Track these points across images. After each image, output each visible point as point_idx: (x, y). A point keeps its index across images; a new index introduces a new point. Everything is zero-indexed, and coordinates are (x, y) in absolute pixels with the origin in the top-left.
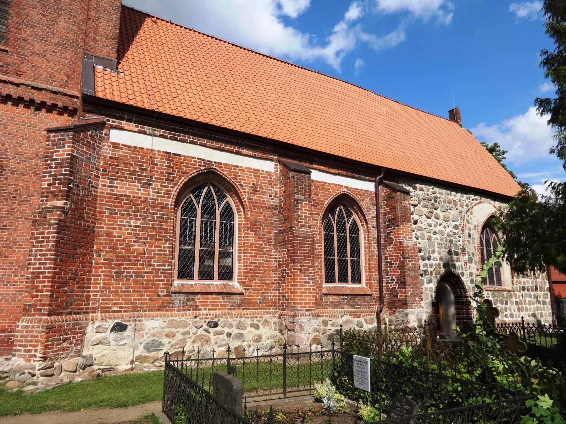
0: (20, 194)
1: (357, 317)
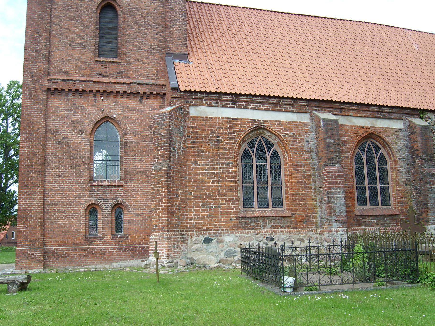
0: (138, 157)
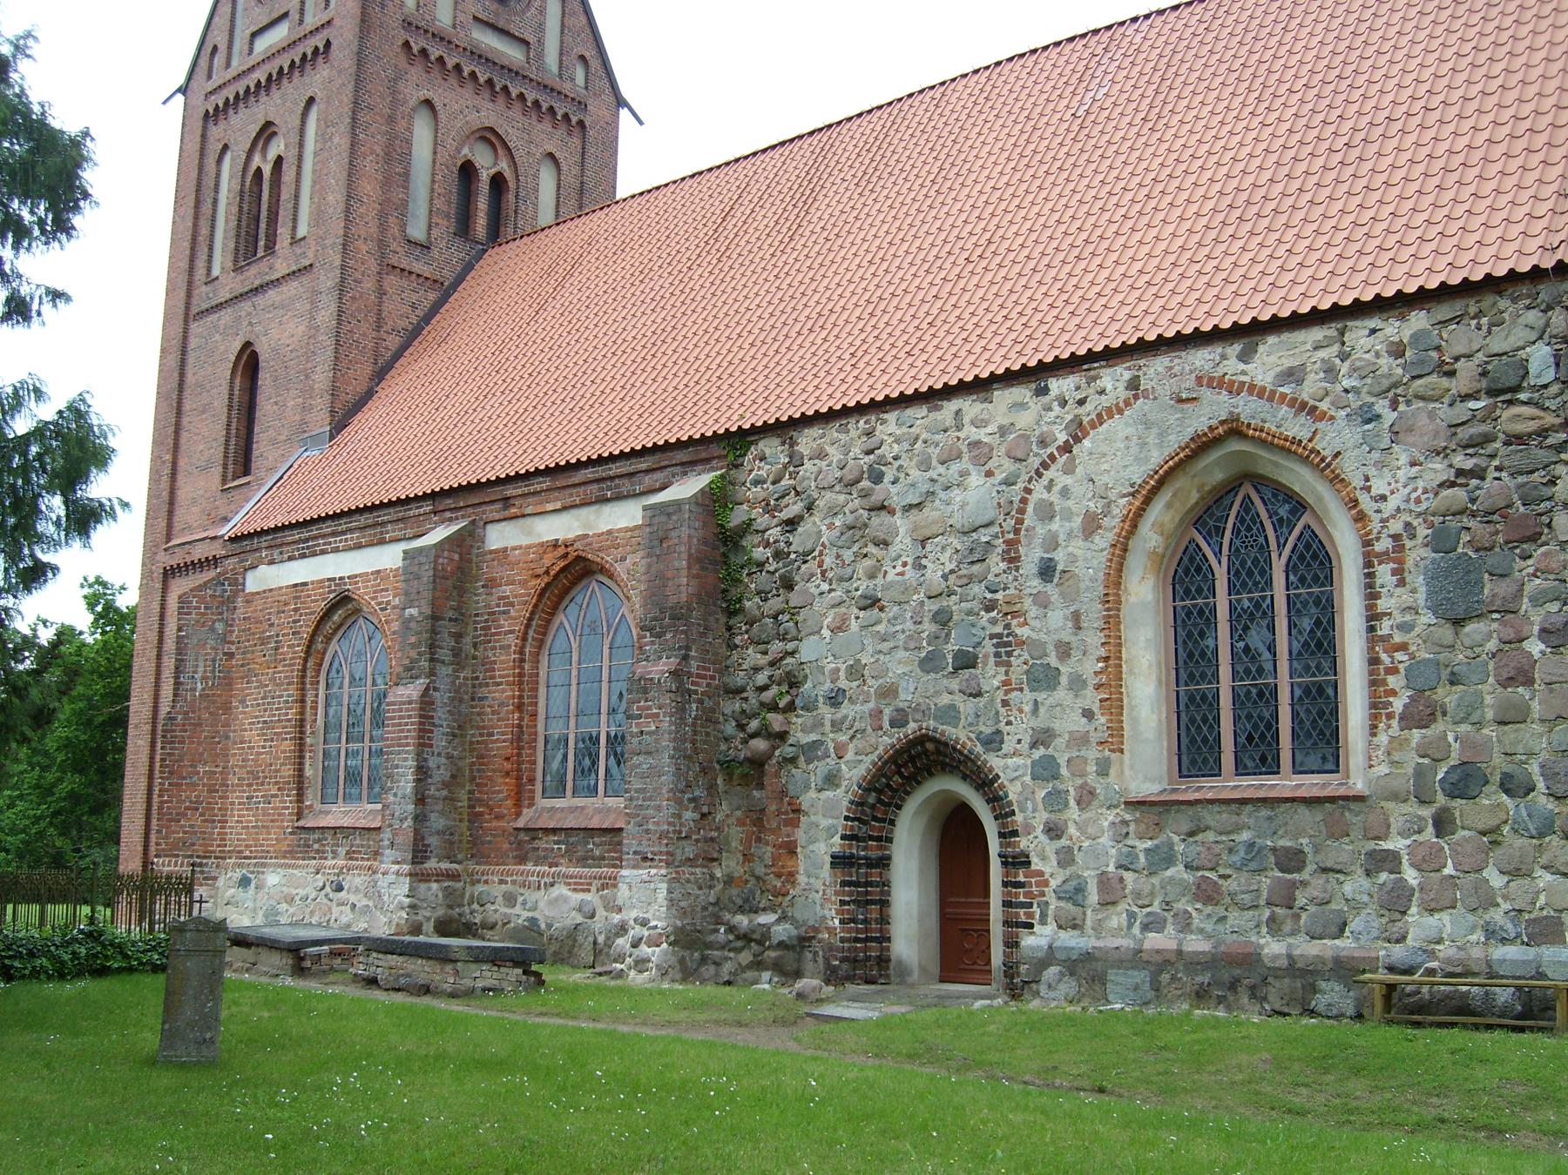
1: (583, 890)
